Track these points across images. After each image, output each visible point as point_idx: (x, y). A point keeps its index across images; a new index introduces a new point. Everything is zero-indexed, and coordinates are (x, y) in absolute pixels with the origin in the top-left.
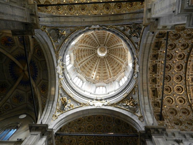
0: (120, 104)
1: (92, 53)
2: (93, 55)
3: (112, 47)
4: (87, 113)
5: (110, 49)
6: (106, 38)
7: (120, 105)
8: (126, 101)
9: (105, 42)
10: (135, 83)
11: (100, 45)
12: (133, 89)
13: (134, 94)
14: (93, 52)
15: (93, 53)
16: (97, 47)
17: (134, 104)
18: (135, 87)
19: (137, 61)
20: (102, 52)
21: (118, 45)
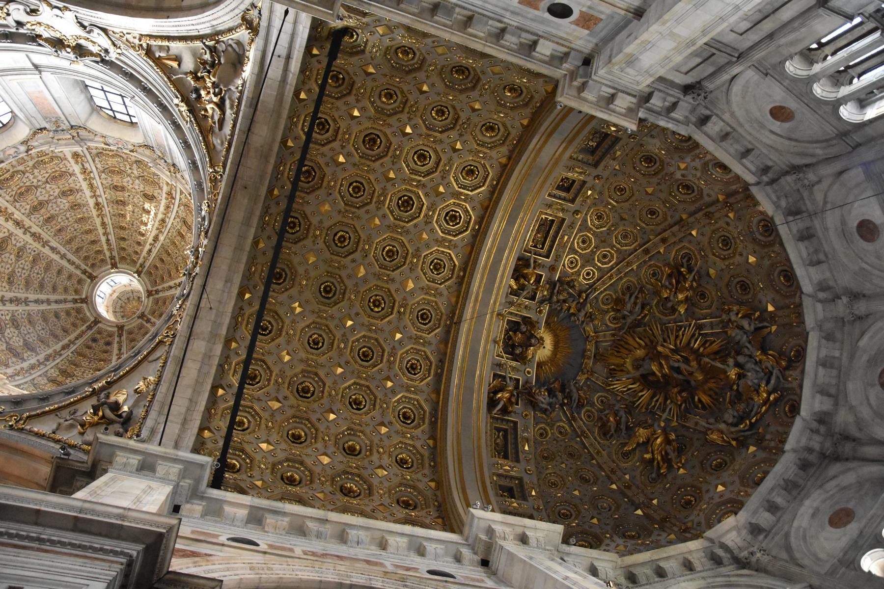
0: (217, 142)
1: (105, 347)
2: (116, 346)
3: (108, 240)
4: (213, 317)
5: (115, 253)
6: (46, 251)
7: (219, 141)
8: (206, 110)
9: (72, 268)
10: (132, 51)
11: (84, 297)
12: (158, 62)
13: (179, 65)
14: (101, 342)
15: (108, 344)
16: (88, 314)
17: (213, 65)
18: (149, 52)
19: (25, 10)
20: (123, 301)
21: (92, 202)
